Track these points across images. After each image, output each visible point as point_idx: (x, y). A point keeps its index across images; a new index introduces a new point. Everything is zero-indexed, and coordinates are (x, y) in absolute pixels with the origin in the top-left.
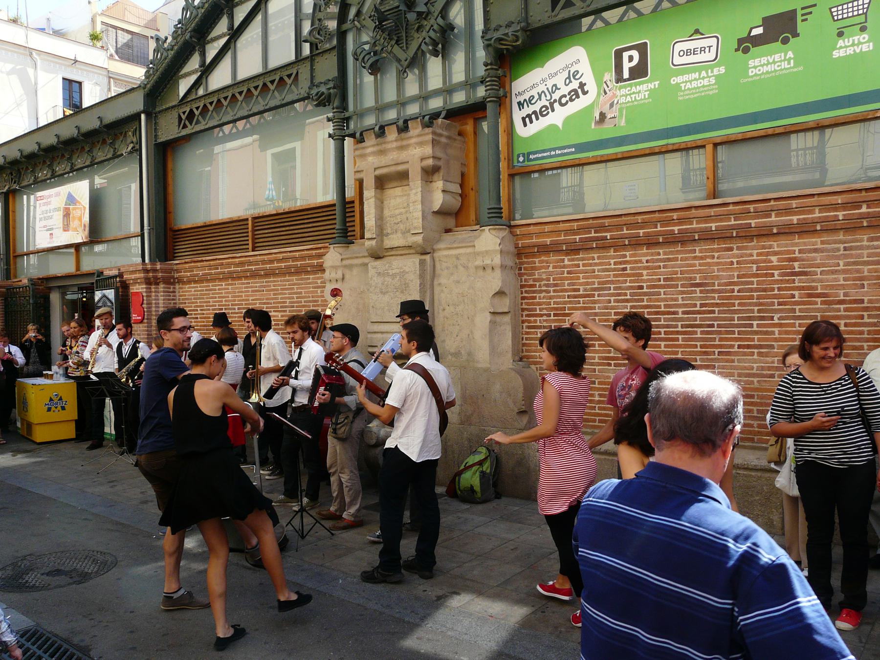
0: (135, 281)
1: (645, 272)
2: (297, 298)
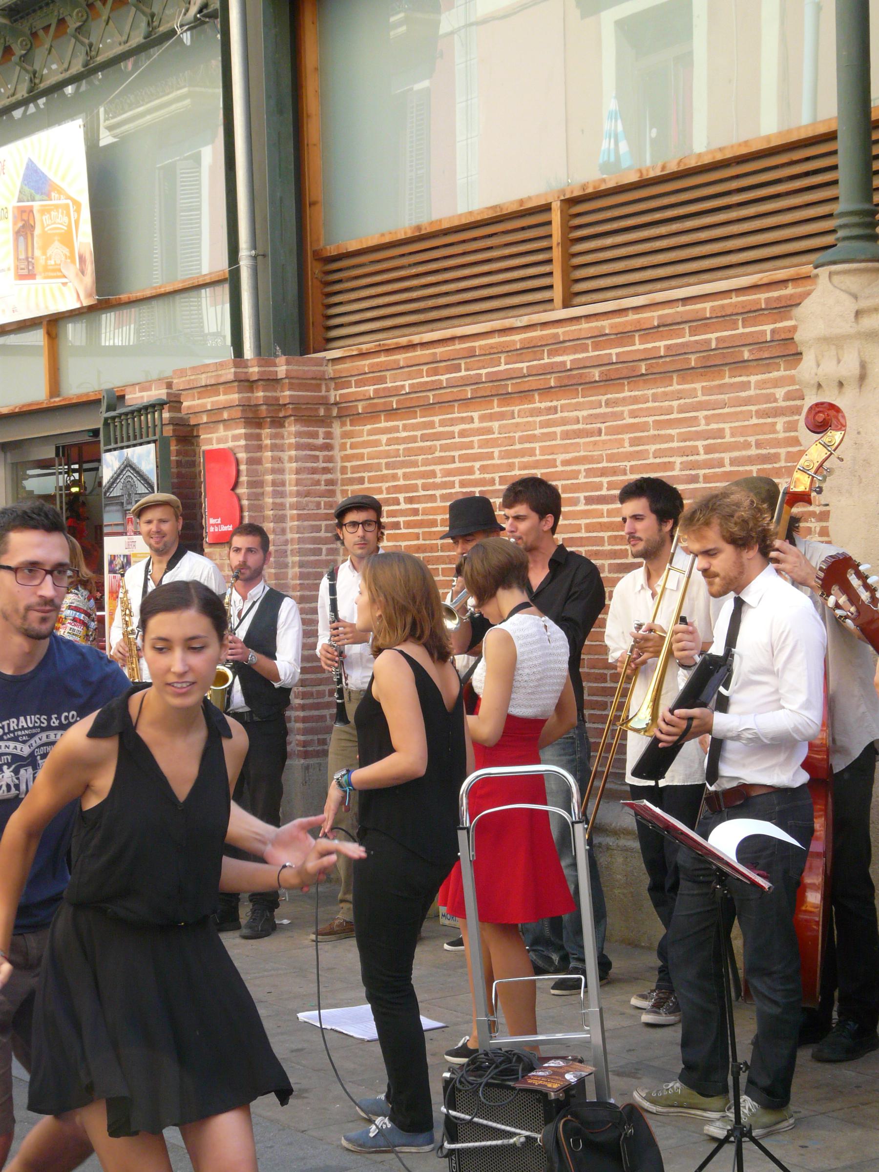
0: (216, 418)
2: (709, 450)
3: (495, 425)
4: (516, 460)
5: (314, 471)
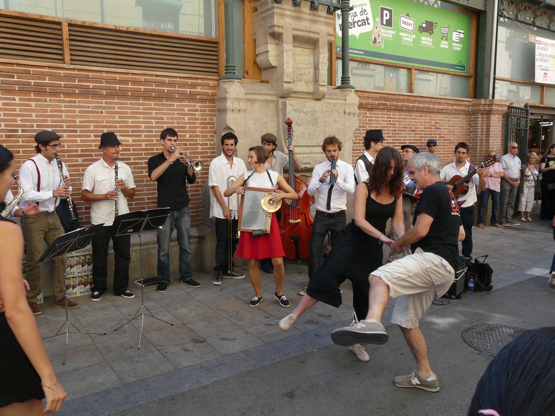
1: (397, 123)
3: (33, 104)
4: (49, 119)
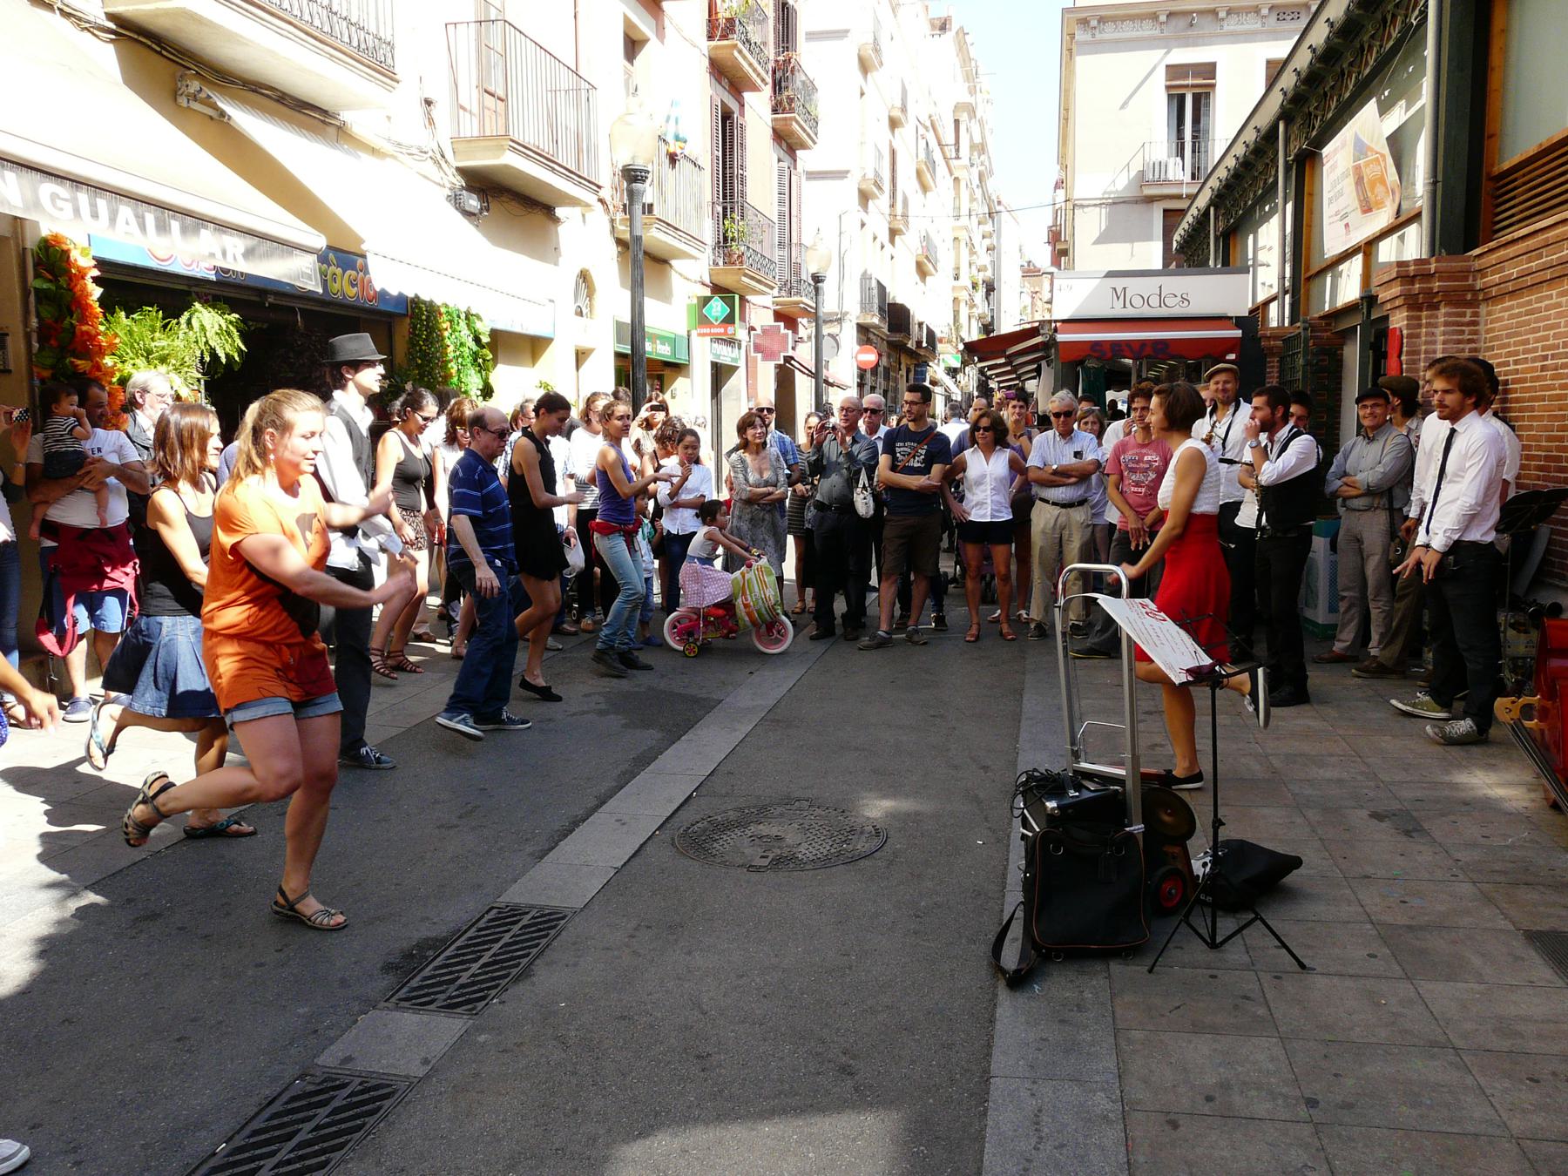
5: (1459, 342)
